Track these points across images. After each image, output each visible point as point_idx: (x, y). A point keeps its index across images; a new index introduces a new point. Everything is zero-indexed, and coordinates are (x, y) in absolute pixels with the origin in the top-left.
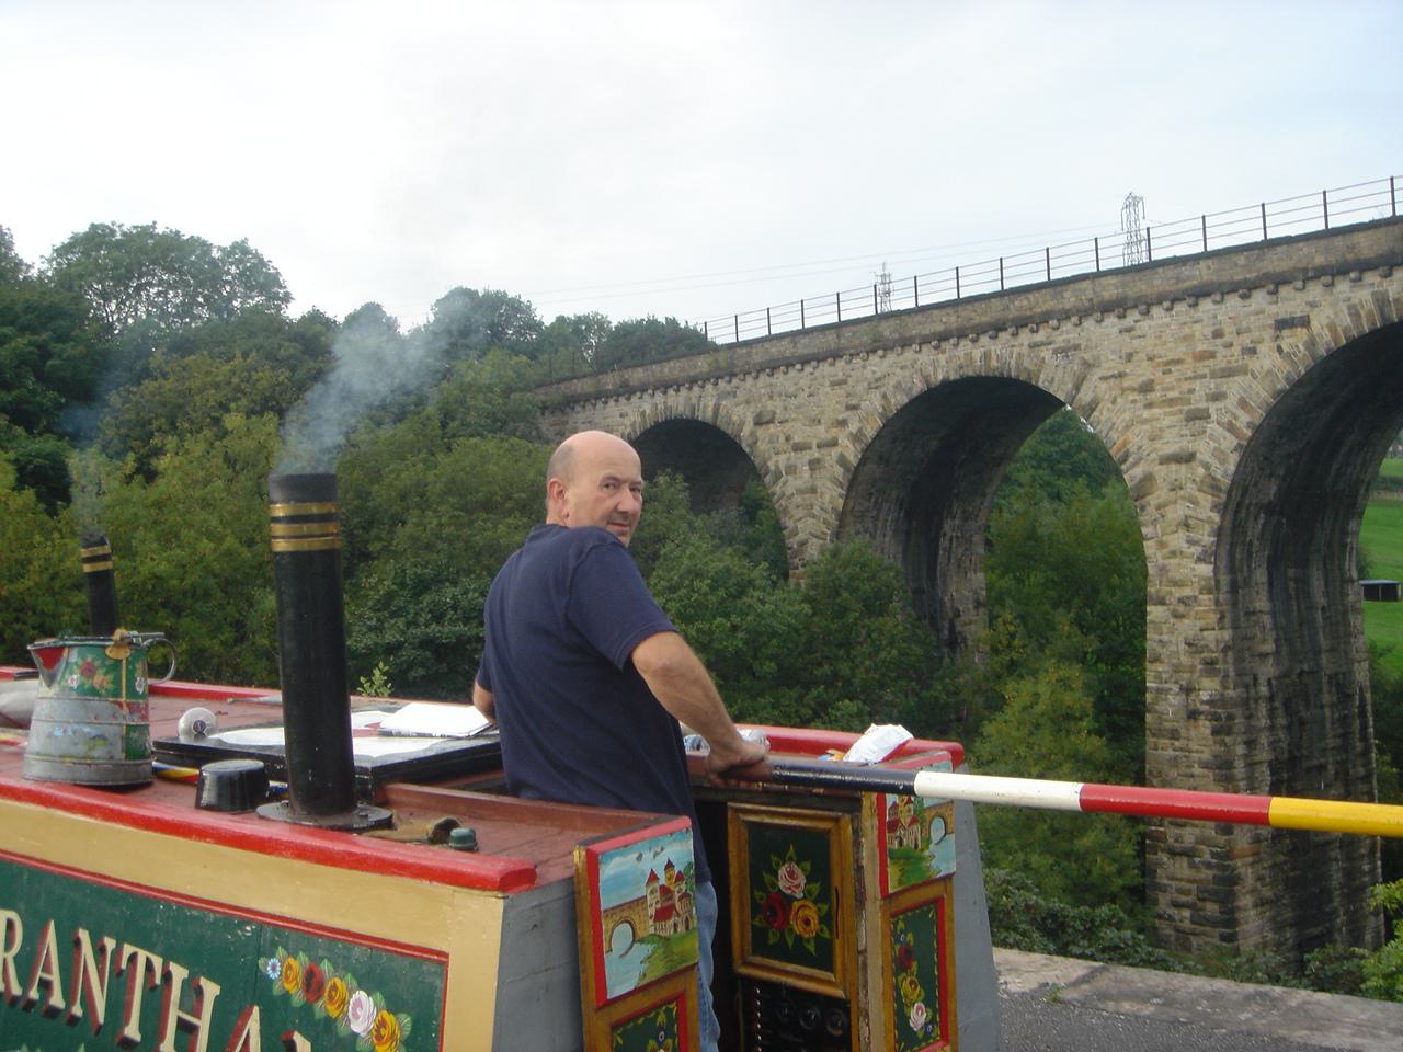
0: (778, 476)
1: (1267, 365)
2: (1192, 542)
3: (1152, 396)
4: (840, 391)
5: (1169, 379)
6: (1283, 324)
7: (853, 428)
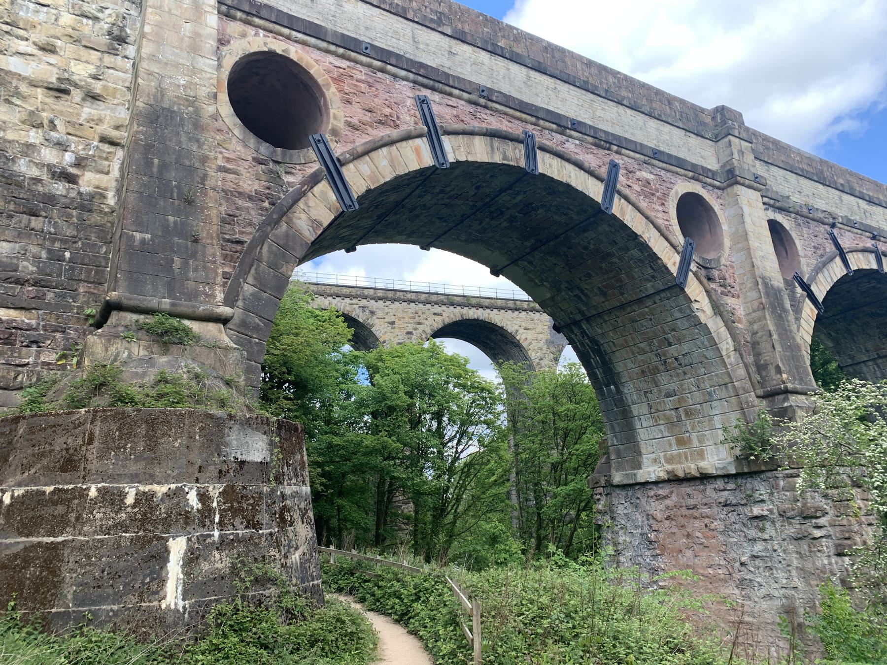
1: (430, 323)
6: (435, 314)
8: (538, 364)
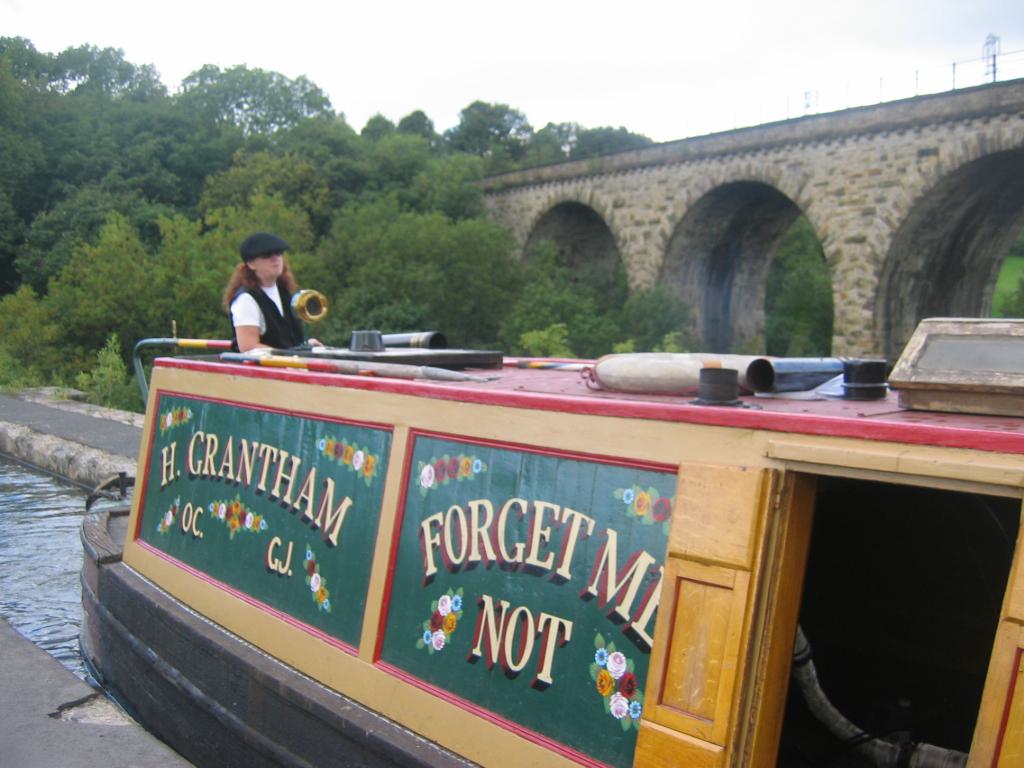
0: (625, 242)
2: (861, 296)
3: (845, 198)
4: (664, 187)
5: (854, 188)
7: (670, 212)
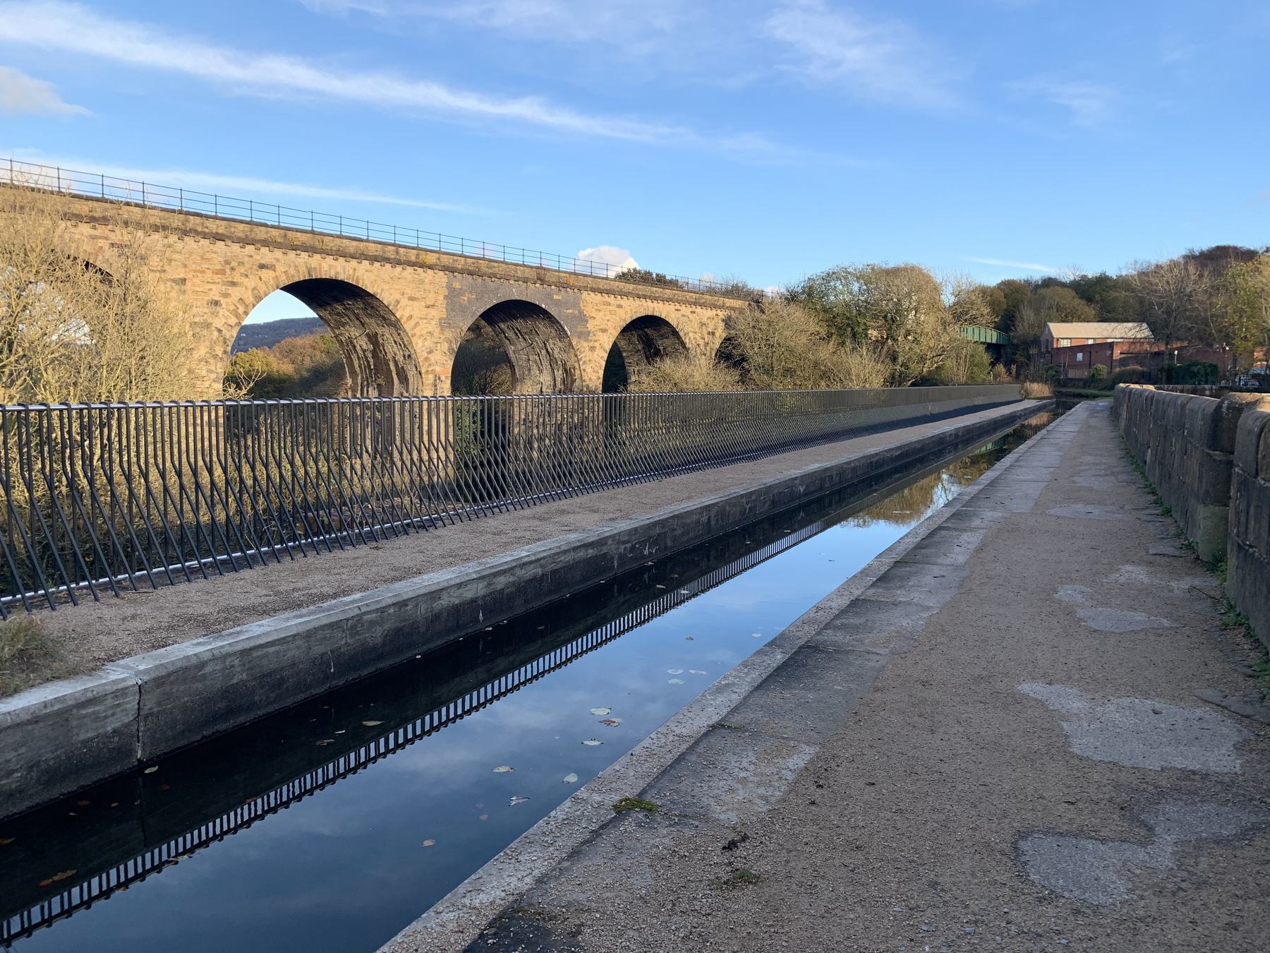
5: (197, 281)
8: (427, 359)
